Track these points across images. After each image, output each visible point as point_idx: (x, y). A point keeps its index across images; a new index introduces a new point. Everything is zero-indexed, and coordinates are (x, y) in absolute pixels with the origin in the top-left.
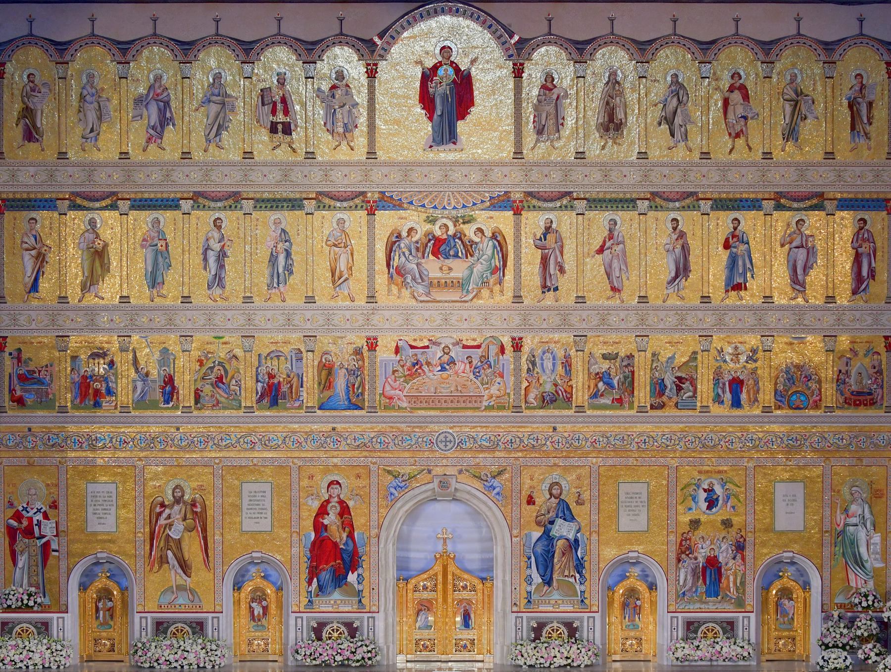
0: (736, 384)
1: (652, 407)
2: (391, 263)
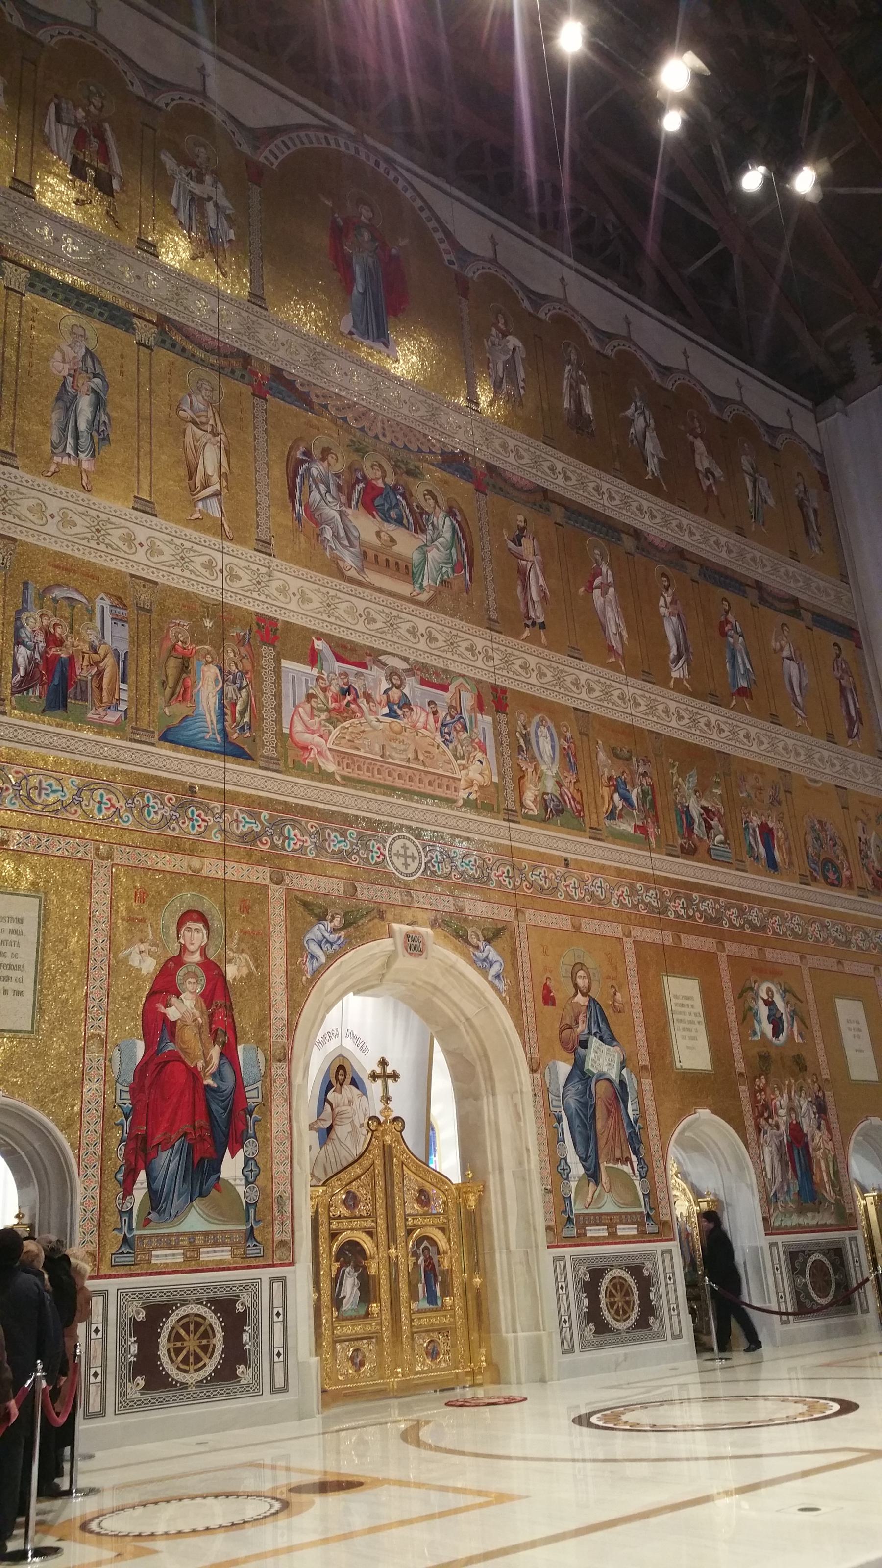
2: (298, 494)
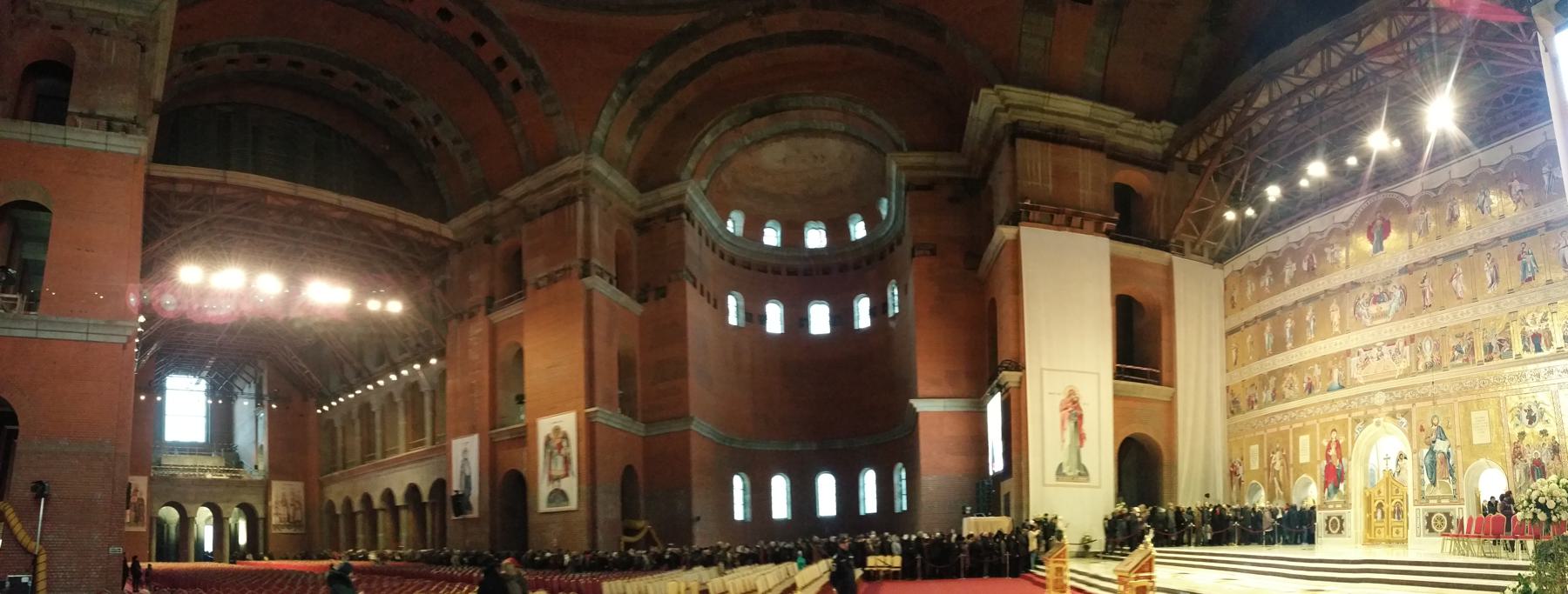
0: (1536, 338)
1: (1486, 361)
